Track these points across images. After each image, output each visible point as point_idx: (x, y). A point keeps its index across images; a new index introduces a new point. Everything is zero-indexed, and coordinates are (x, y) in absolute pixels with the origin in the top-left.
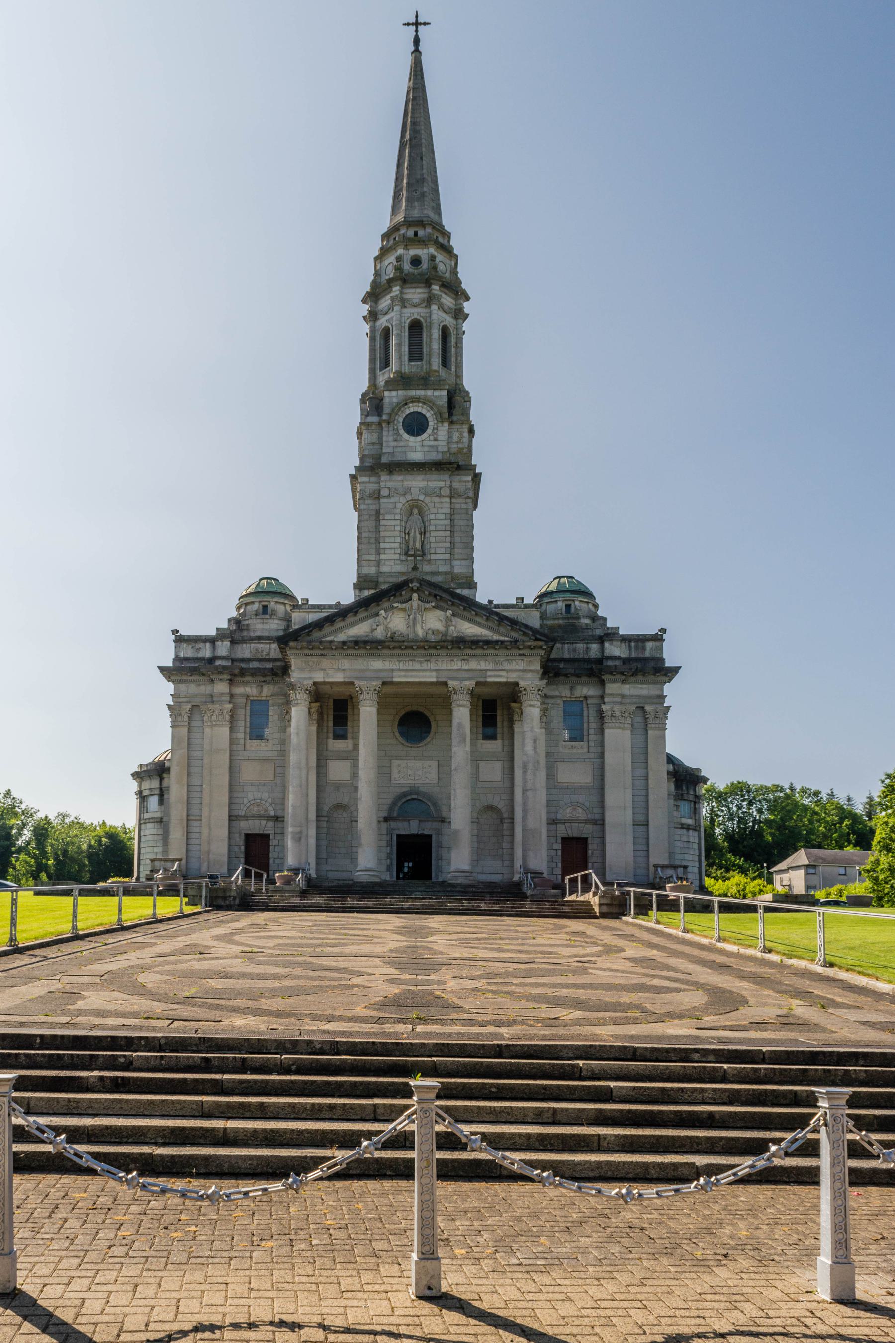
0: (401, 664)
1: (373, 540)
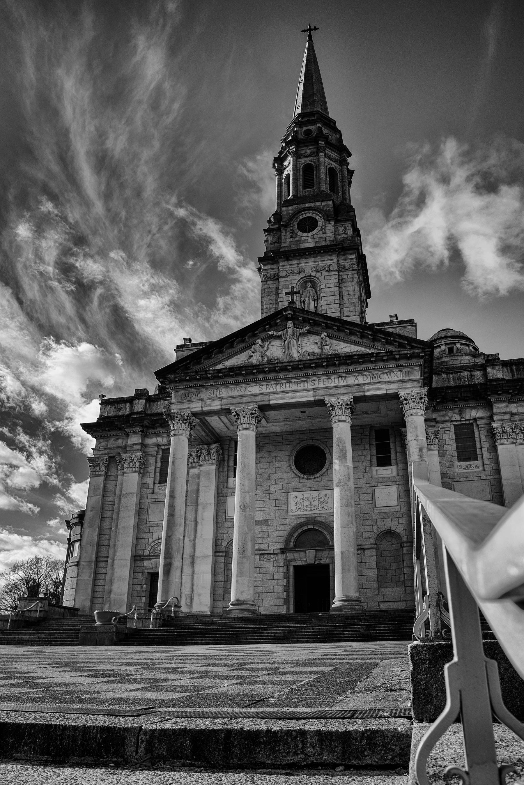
0: (278, 387)
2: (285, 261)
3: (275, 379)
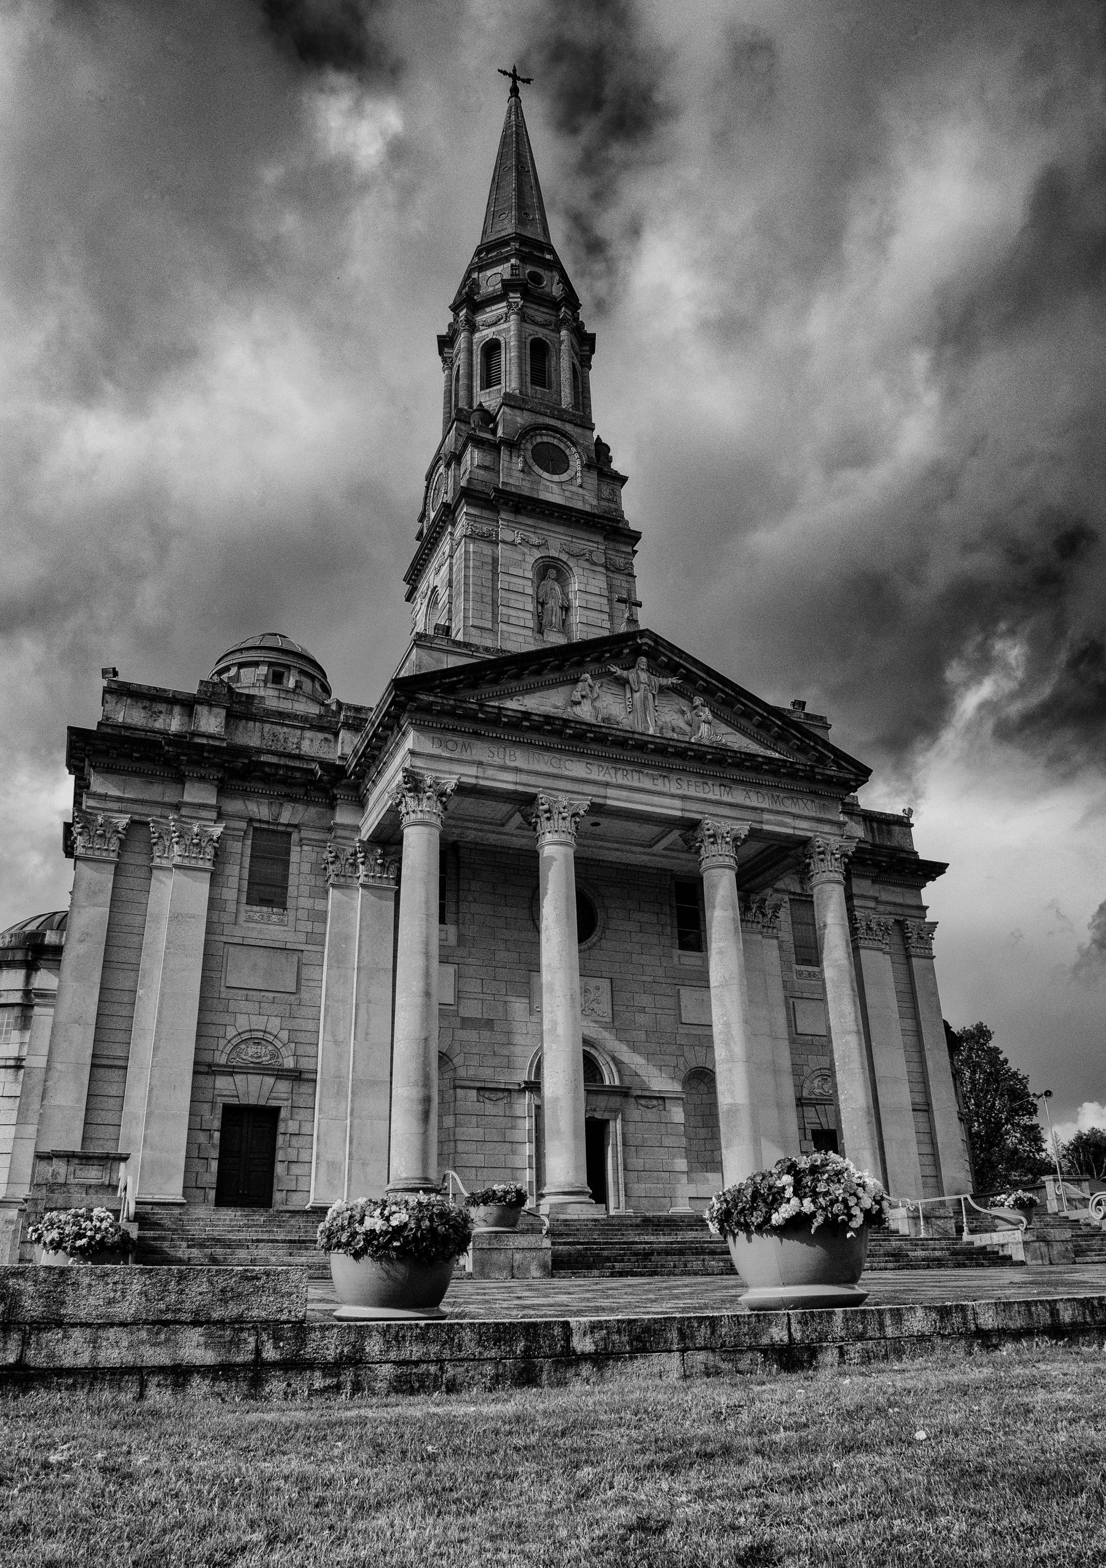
1: (488, 600)
2: (511, 512)
3: (616, 760)
